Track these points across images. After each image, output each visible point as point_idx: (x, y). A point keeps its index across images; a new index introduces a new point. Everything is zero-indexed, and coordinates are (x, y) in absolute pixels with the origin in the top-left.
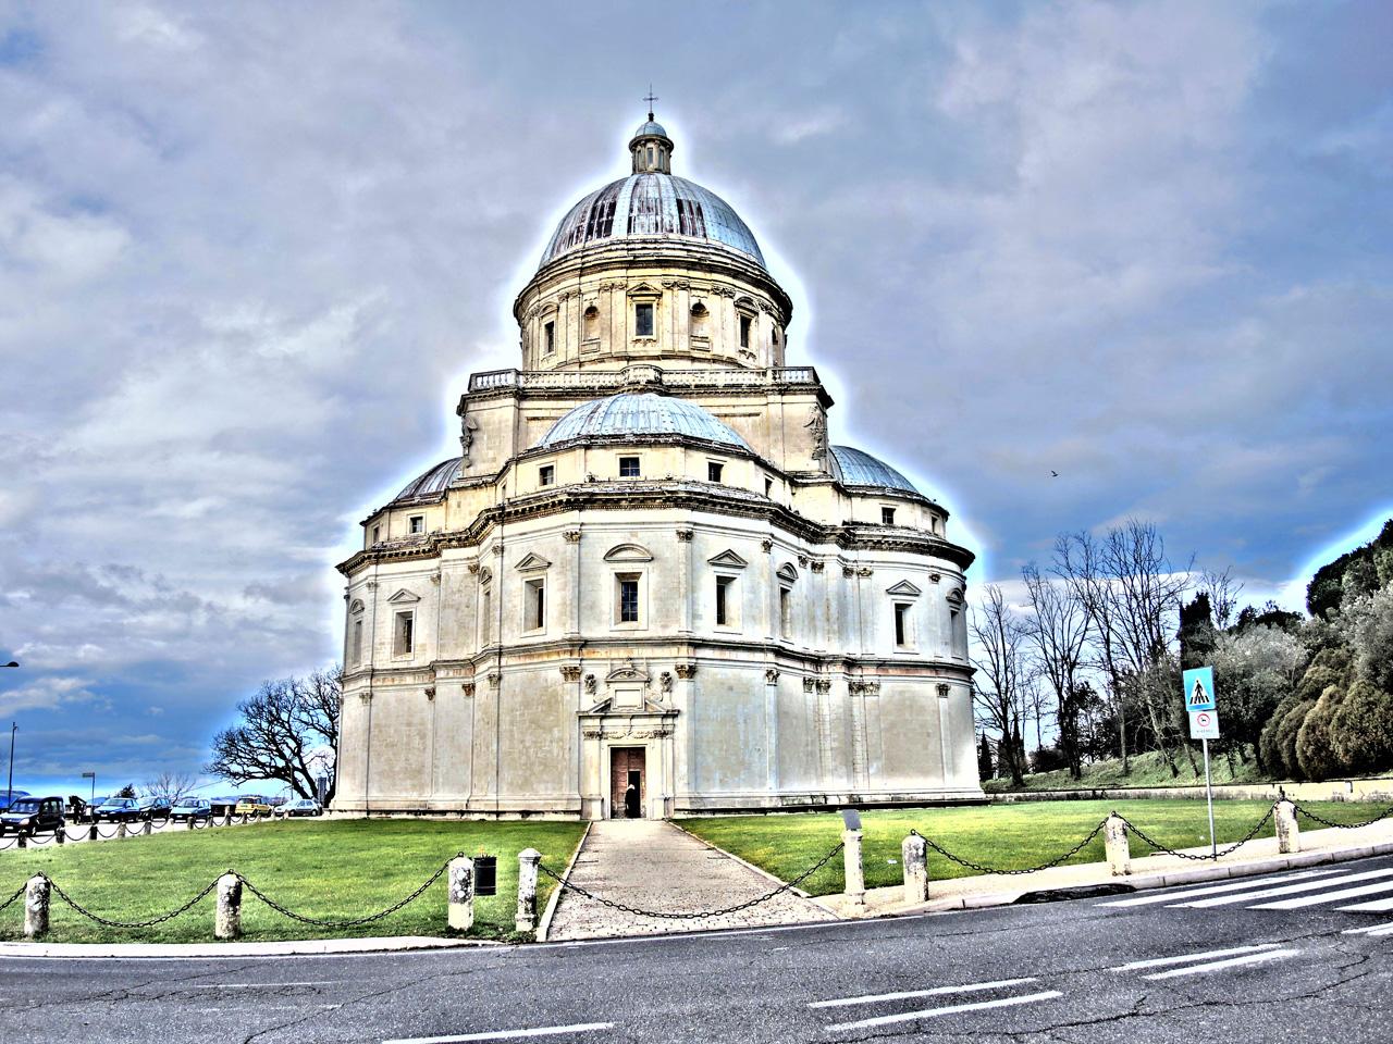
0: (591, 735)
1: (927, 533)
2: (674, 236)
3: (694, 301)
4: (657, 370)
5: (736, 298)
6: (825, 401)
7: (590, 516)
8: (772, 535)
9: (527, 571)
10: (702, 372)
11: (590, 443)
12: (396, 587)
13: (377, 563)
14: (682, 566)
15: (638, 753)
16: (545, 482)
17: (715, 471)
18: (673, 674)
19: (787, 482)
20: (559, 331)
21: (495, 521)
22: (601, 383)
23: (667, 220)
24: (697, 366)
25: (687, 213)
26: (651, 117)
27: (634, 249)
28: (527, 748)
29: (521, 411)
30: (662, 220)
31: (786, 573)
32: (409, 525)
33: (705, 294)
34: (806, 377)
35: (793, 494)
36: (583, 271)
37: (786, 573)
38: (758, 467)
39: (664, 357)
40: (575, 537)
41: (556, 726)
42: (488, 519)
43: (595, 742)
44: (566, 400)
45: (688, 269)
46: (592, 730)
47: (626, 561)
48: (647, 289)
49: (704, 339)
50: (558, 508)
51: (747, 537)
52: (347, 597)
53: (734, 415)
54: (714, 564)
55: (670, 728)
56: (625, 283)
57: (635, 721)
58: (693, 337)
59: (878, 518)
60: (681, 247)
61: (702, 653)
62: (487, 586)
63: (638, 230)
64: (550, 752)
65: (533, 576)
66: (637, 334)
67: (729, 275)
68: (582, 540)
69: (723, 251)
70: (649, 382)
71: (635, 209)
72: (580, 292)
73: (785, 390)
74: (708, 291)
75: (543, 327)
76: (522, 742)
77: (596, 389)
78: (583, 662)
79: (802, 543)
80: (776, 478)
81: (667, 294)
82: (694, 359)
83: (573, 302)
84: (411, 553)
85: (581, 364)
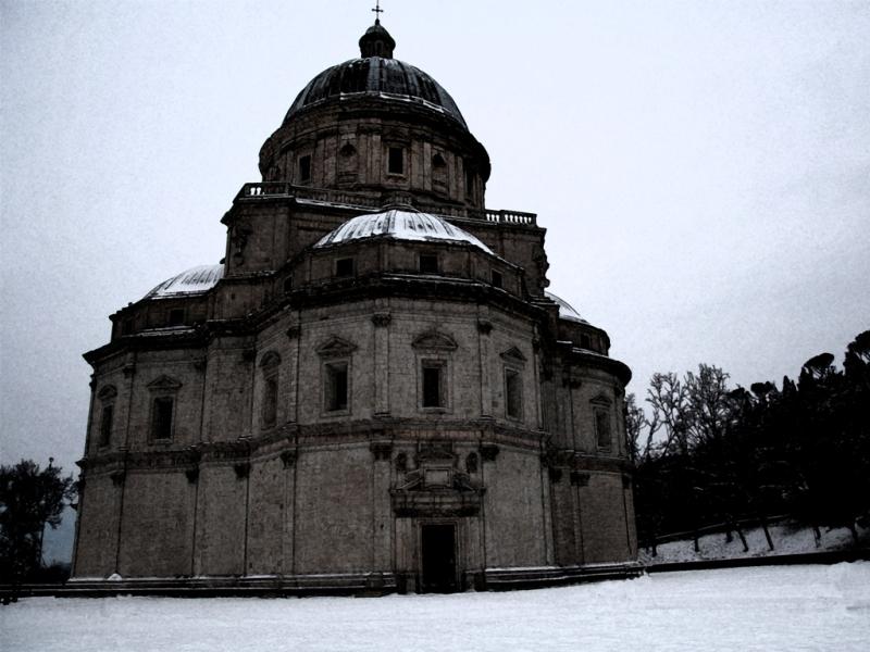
3: (435, 152)
7: (395, 302)
12: (155, 373)
15: (448, 531)
18: (478, 454)
26: (377, 22)
43: (409, 520)
49: (442, 184)
52: (93, 385)
57: (444, 500)
58: (435, 182)
65: (335, 361)
72: (337, 133)
81: (415, 147)
82: (436, 199)
83: (331, 140)
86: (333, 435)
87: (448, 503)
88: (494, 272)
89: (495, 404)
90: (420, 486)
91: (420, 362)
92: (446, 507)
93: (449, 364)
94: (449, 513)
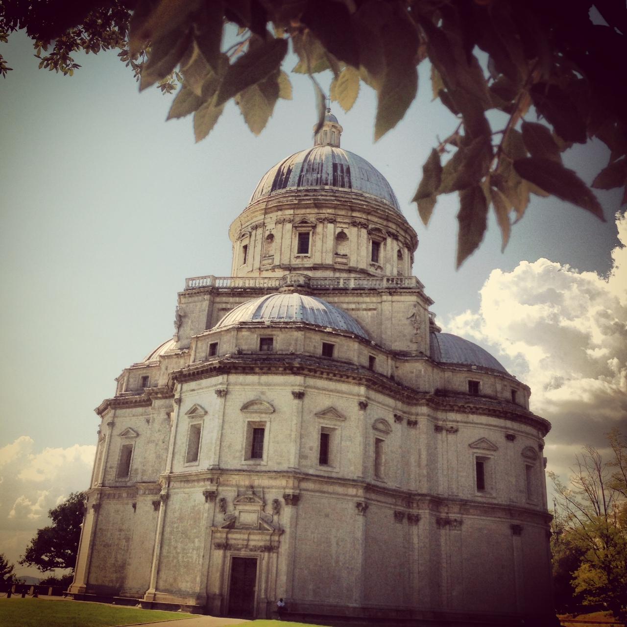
0: (219, 546)
1: (507, 401)
3: (338, 230)
4: (306, 276)
5: (370, 226)
6: (428, 301)
7: (233, 378)
9: (193, 418)
10: (338, 278)
13: (115, 409)
14: (294, 418)
17: (328, 349)
18: (282, 500)
19: (390, 361)
20: (250, 251)
21: (177, 380)
22: (270, 286)
23: (324, 176)
24: (337, 275)
25: (339, 172)
27: (300, 196)
28: (178, 553)
29: (215, 305)
30: (321, 177)
31: (381, 426)
32: (141, 381)
34: (413, 284)
35: (397, 367)
36: (267, 211)
37: (381, 426)
38: (362, 347)
39: (315, 268)
40: (222, 393)
41: (197, 537)
44: (244, 297)
45: (335, 208)
46: (217, 541)
48: (306, 222)
49: (345, 256)
50: (214, 373)
51: (346, 395)
53: (358, 310)
54: (320, 417)
55: (276, 544)
56: (292, 218)
57: (252, 537)
59: (465, 388)
60: (332, 194)
61: (304, 485)
63: (305, 183)
64: (191, 557)
66: (298, 253)
67: (364, 212)
68: (228, 396)
69: (361, 195)
70: (300, 286)
71: (305, 170)
72: (264, 225)
73: (394, 292)
74: (349, 224)
75: (242, 248)
76: (176, 548)
77: (266, 289)
78: (220, 488)
79: (399, 405)
80: (380, 355)
81: (320, 228)
82: (335, 270)
83: (260, 231)
84: (136, 401)
86: (188, 481)
87: (255, 540)
89: (302, 456)
90: (231, 525)
91: (246, 423)
92: (252, 543)
93: (268, 425)
94: (255, 549)
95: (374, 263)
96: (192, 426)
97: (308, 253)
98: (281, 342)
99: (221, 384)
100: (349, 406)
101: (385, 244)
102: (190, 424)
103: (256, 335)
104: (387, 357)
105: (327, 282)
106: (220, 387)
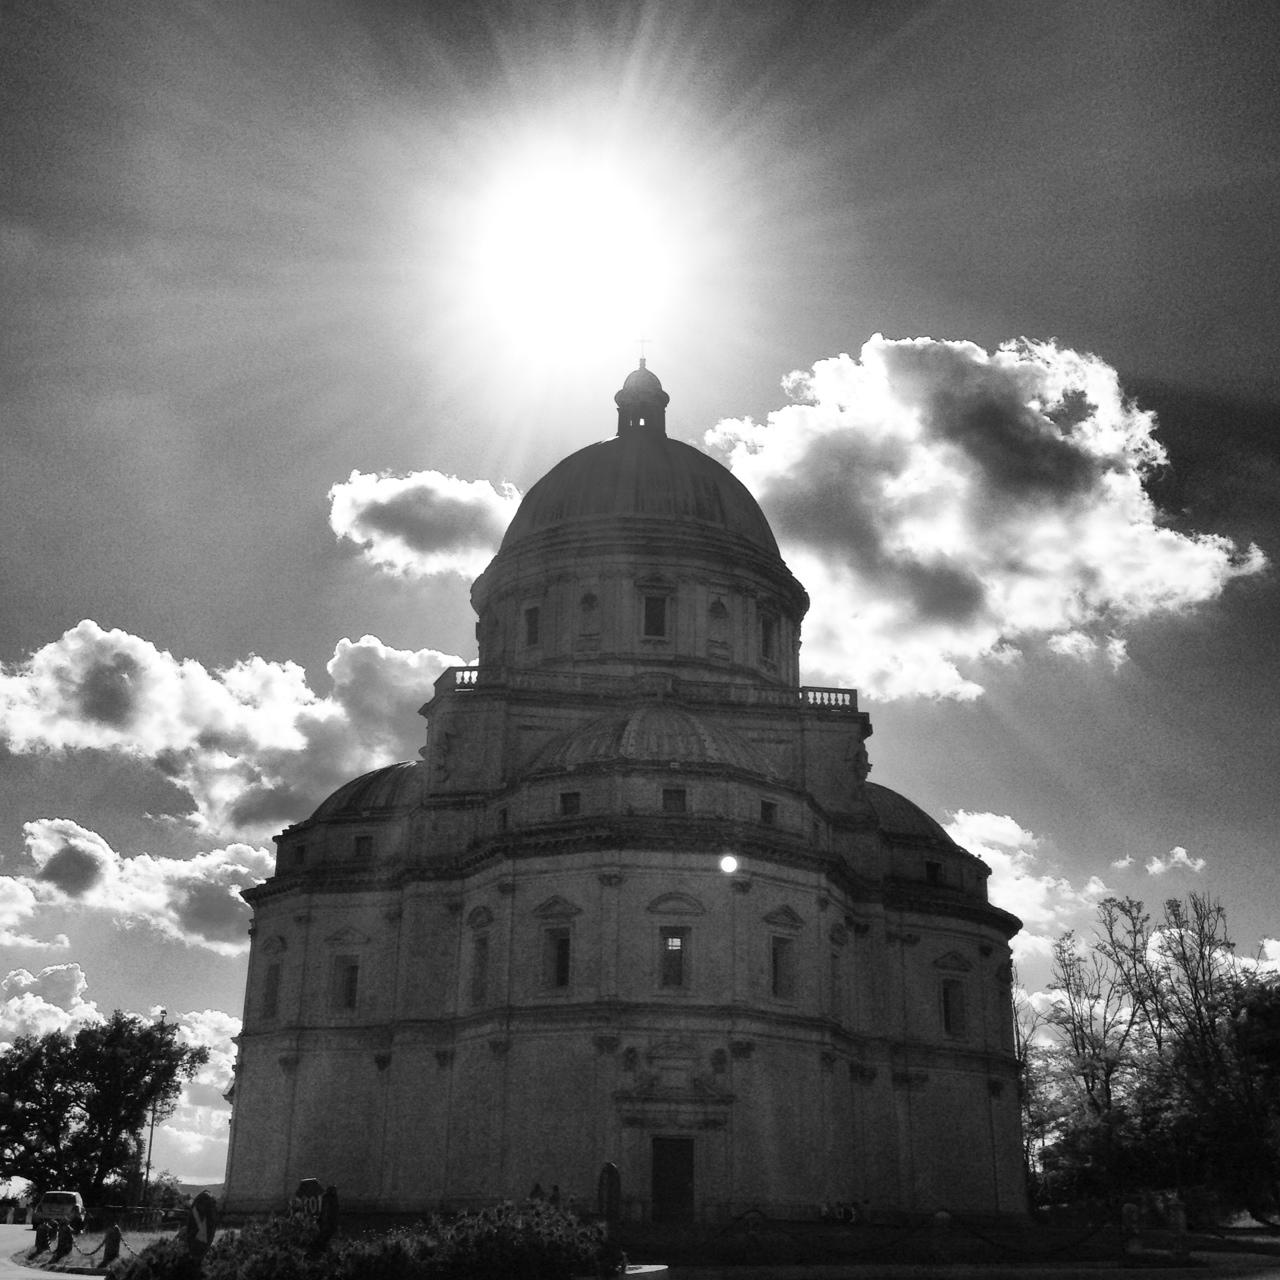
2: (688, 518)
3: (713, 598)
5: (762, 594)
8: (829, 891)
11: (628, 767)
13: (310, 891)
16: (566, 810)
17: (768, 809)
19: (830, 831)
31: (836, 935)
33: (725, 591)
37: (836, 935)
42: (493, 852)
47: (675, 913)
49: (724, 645)
54: (768, 922)
62: (485, 929)
66: (647, 634)
70: (667, 695)
82: (710, 668)
85: (576, 663)
88: (763, 803)
95: (765, 659)
96: (547, 930)
97: (663, 635)
98: (699, 797)
99: (611, 864)
100: (806, 906)
101: (779, 627)
102: (543, 928)
103: (655, 785)
104: (828, 825)
105: (704, 691)
106: (606, 870)
